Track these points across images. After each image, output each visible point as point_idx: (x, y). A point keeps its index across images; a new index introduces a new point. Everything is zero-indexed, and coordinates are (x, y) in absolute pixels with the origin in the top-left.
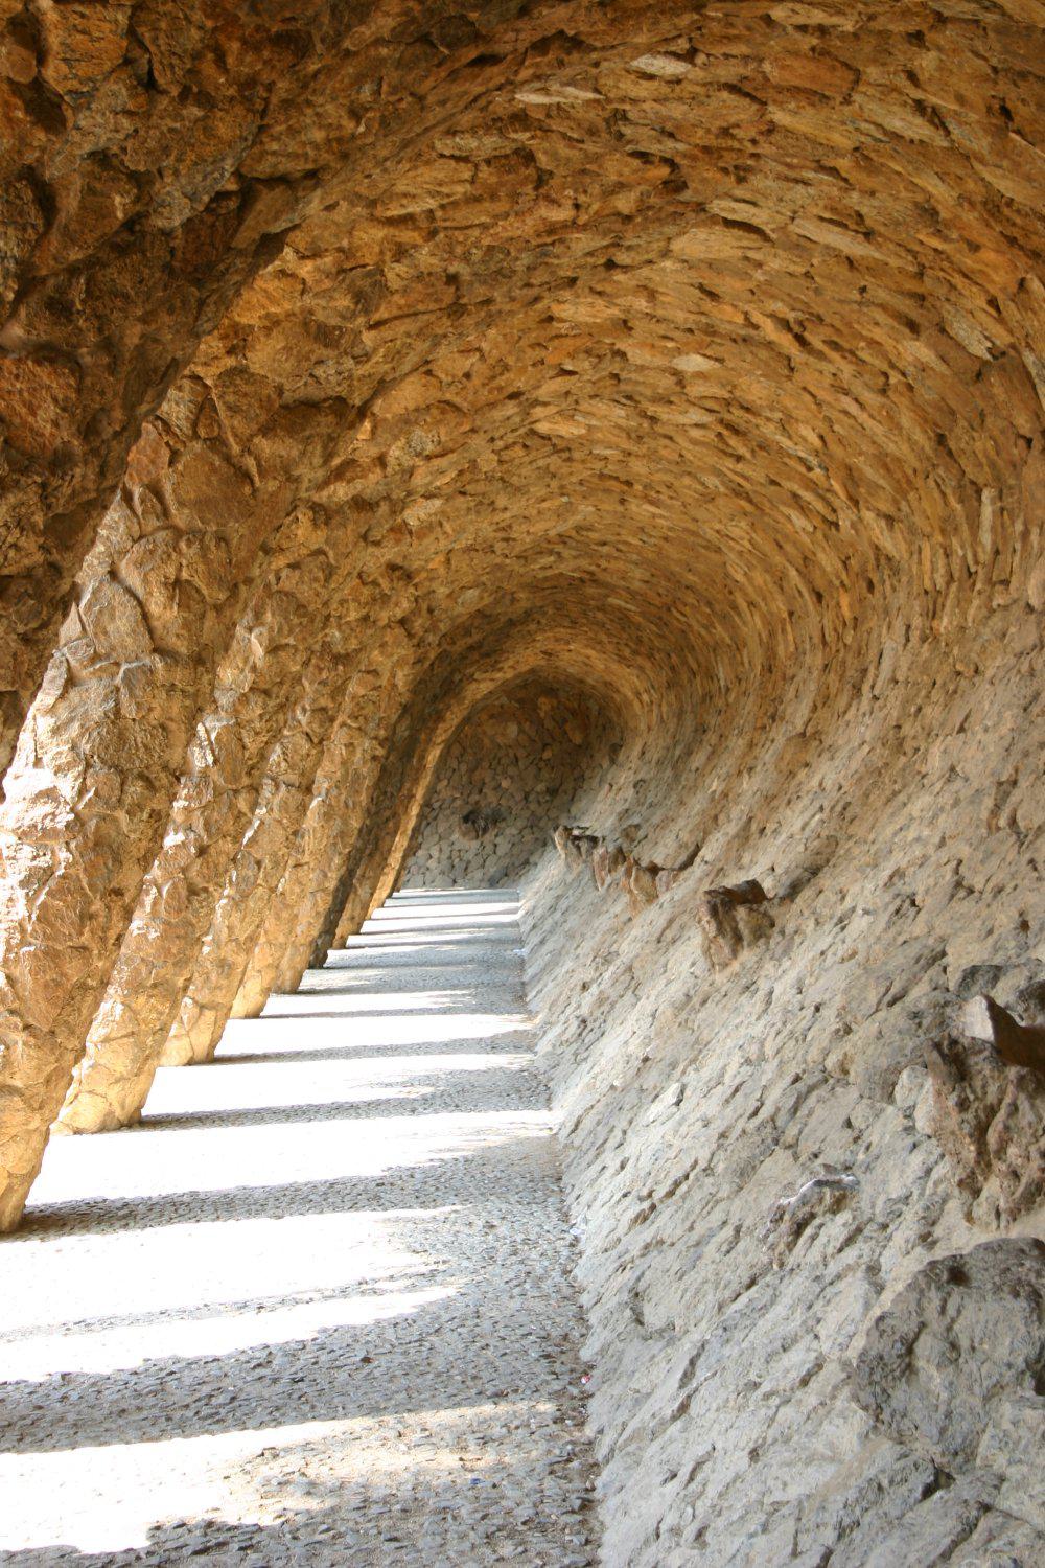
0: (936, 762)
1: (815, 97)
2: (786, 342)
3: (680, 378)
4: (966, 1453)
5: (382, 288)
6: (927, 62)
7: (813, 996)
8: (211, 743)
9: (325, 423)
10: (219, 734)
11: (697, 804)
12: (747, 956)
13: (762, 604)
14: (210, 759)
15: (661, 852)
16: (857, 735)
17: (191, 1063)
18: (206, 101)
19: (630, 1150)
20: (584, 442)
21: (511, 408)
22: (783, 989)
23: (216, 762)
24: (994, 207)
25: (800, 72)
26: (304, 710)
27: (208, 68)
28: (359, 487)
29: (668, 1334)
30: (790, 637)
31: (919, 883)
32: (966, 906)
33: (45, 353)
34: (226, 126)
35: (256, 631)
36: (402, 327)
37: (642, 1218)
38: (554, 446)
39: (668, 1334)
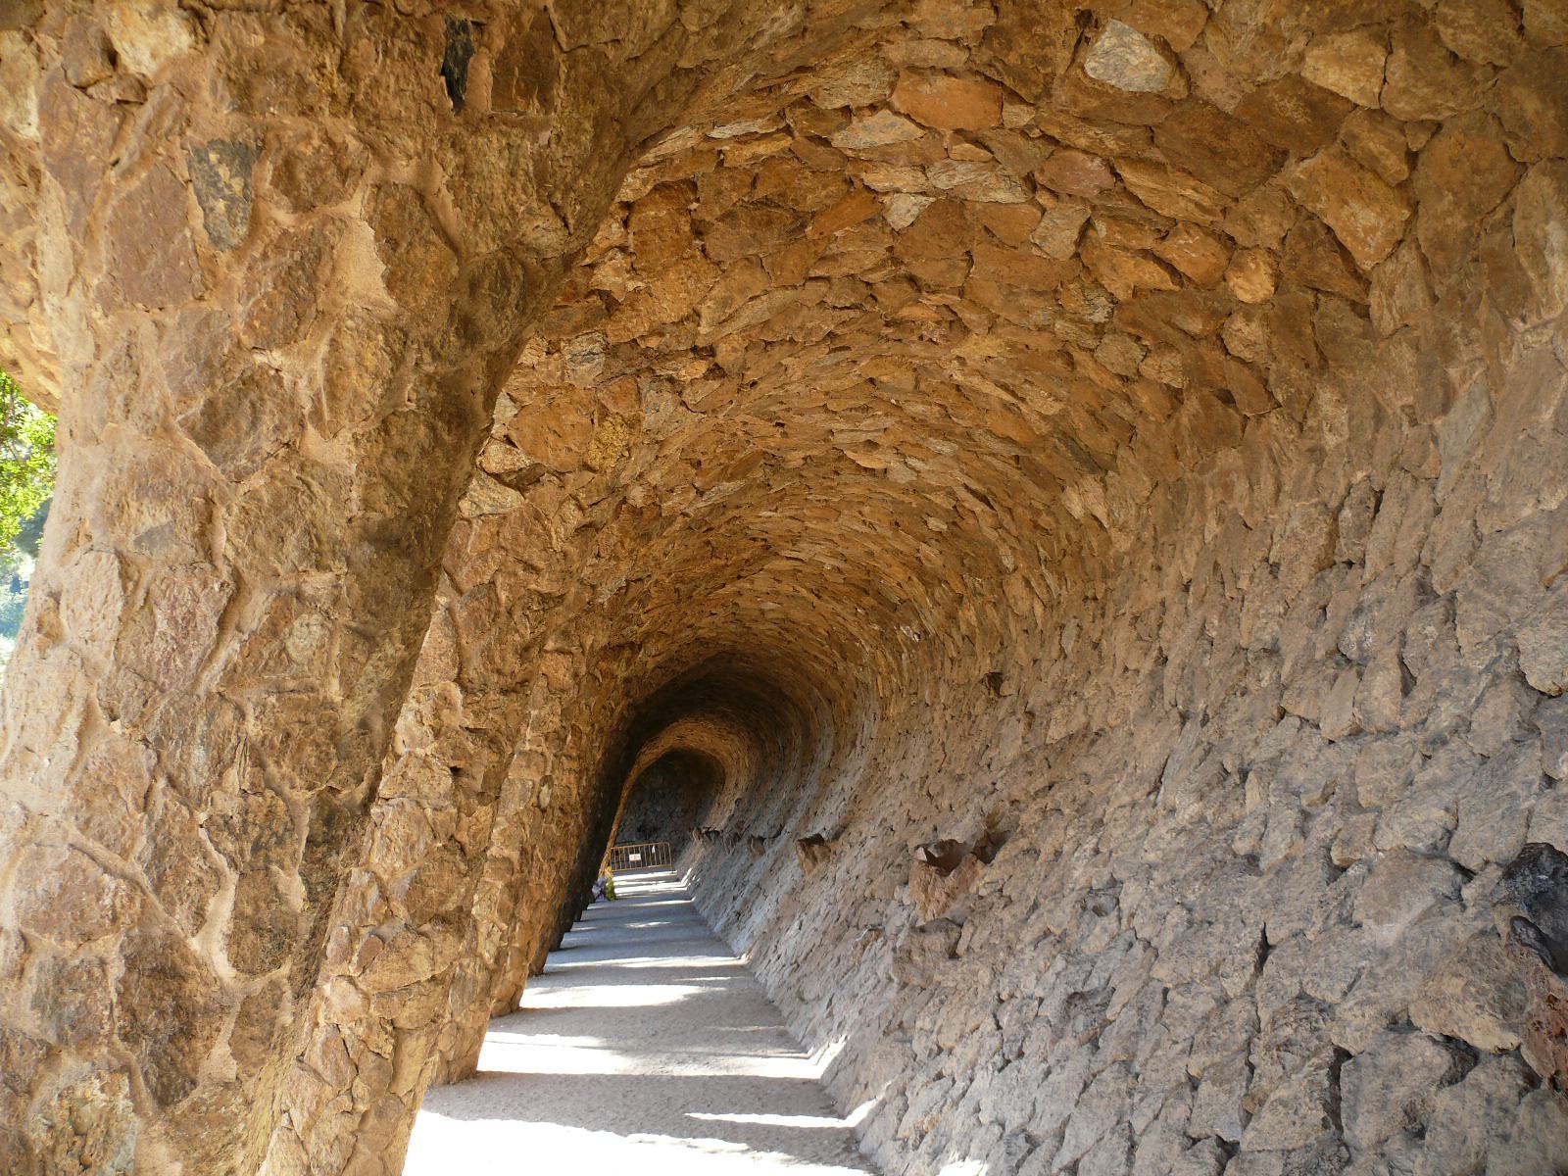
0: (893, 772)
1: (820, 519)
2: (812, 598)
3: (763, 612)
4: (930, 979)
5: (649, 597)
6: (866, 510)
7: (854, 873)
9: (627, 653)
11: (776, 806)
12: (821, 866)
15: (762, 830)
16: (856, 765)
18: (617, 559)
19: (781, 950)
21: (689, 632)
22: (841, 874)
24: (897, 552)
25: (818, 513)
27: (619, 547)
29: (818, 998)
31: (894, 822)
32: (913, 827)
33: (560, 651)
34: (624, 567)
36: (656, 612)
37: (794, 971)
39: (818, 998)
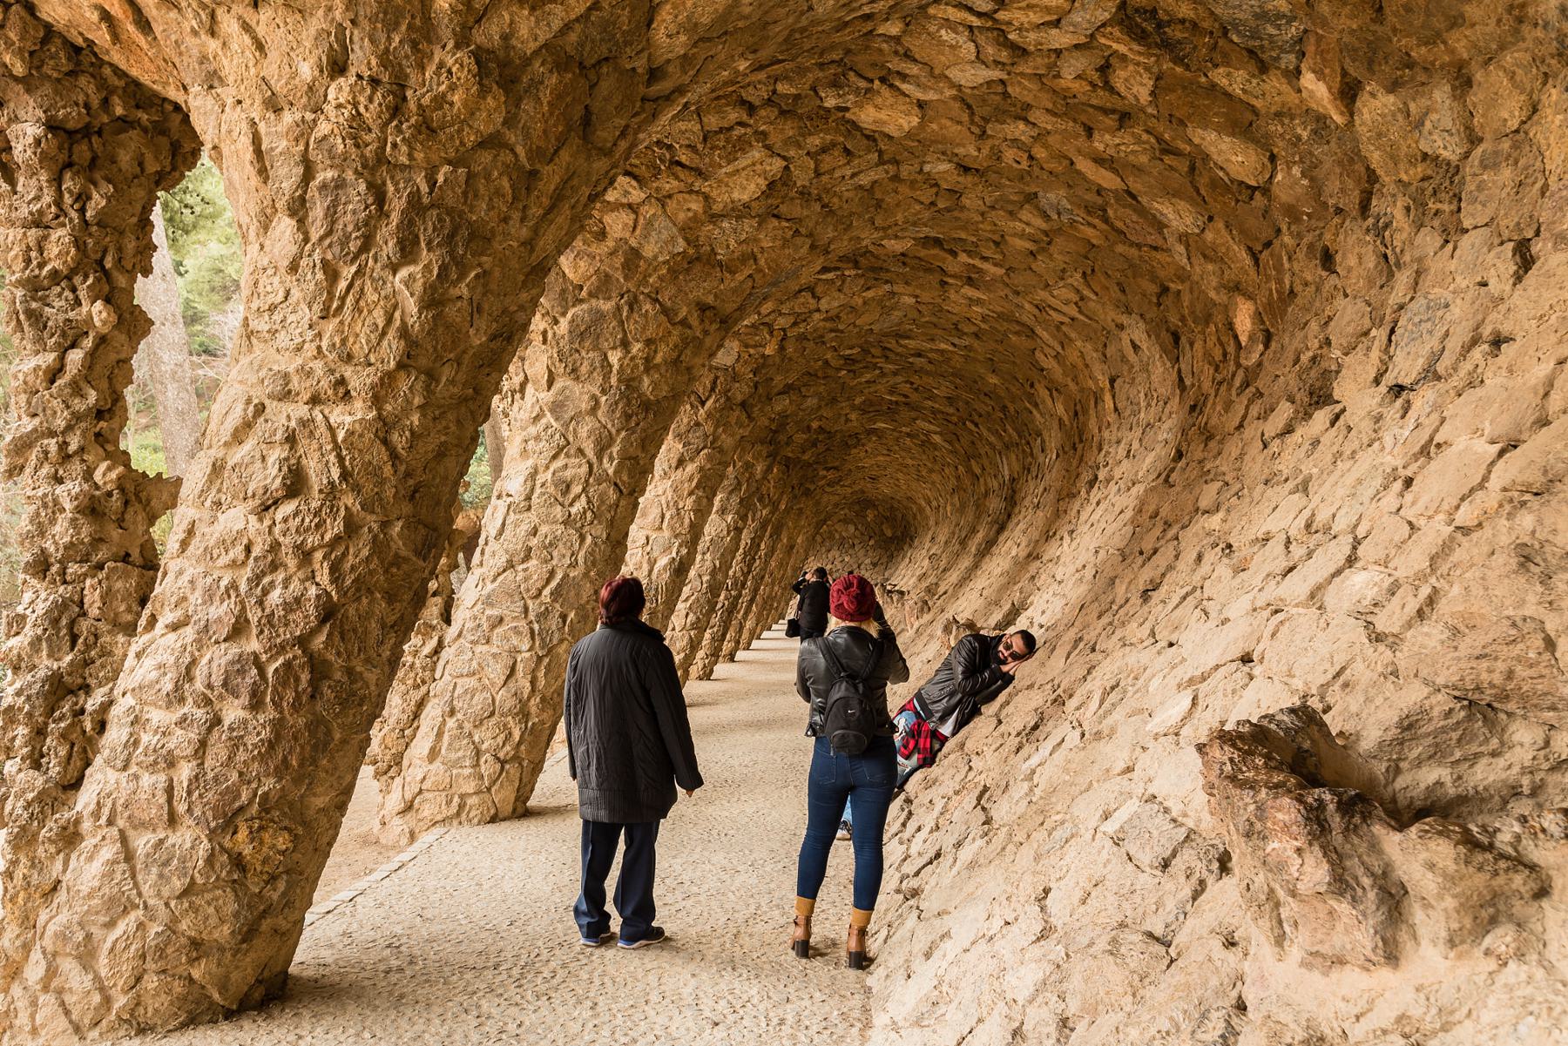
8: (337, 447)
10: (350, 433)
13: (1072, 386)
14: (335, 473)
17: (494, 820)
20: (918, 143)
23: (345, 475)
26: (611, 459)
28: (557, 24)
30: (1109, 403)
35: (403, 273)
38: (881, 153)
